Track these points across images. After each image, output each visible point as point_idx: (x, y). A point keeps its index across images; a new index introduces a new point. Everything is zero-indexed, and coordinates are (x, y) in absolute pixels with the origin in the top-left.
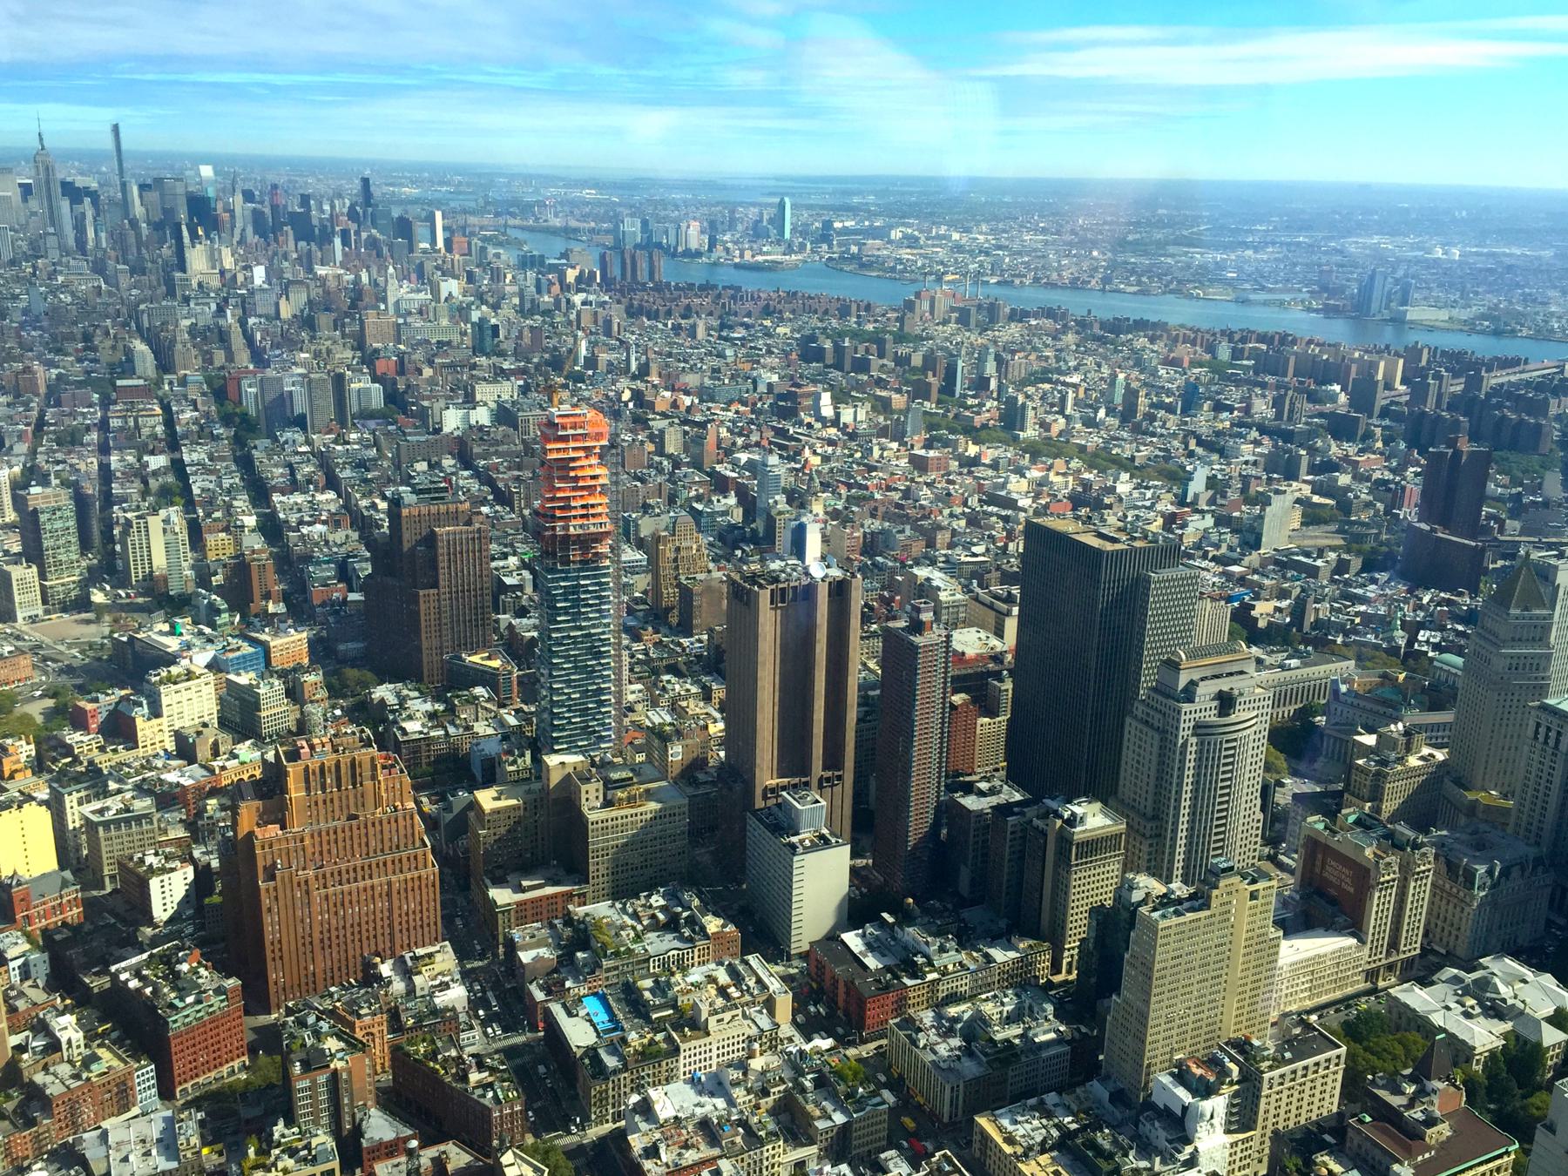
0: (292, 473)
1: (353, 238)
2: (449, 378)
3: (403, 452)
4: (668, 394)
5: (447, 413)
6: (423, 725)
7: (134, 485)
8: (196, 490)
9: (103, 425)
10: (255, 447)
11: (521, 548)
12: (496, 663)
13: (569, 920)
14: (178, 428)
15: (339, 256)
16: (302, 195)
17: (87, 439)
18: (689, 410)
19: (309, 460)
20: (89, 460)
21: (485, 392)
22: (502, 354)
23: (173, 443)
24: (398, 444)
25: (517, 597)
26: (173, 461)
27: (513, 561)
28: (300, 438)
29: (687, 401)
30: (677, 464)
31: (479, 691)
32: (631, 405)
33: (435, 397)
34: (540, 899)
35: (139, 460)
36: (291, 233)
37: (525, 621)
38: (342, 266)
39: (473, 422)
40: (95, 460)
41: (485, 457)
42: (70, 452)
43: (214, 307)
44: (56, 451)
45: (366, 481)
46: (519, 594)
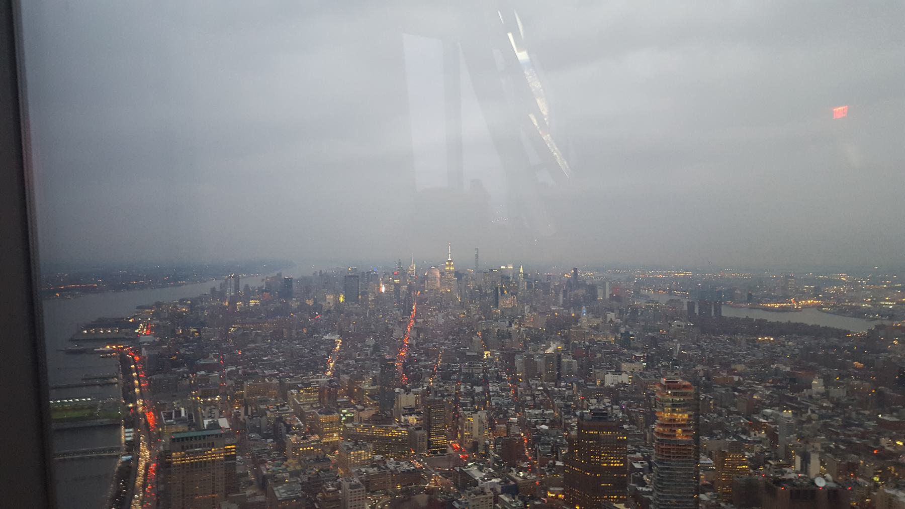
0: (534, 399)
7: (469, 399)
8: (493, 404)
10: (519, 386)
15: (561, 302)
17: (452, 377)
19: (542, 394)
20: (453, 386)
21: (625, 366)
23: (485, 382)
27: (639, 455)
29: (736, 378)
37: (644, 489)
38: (563, 306)
43: (508, 322)
44: (441, 382)
46: (641, 473)
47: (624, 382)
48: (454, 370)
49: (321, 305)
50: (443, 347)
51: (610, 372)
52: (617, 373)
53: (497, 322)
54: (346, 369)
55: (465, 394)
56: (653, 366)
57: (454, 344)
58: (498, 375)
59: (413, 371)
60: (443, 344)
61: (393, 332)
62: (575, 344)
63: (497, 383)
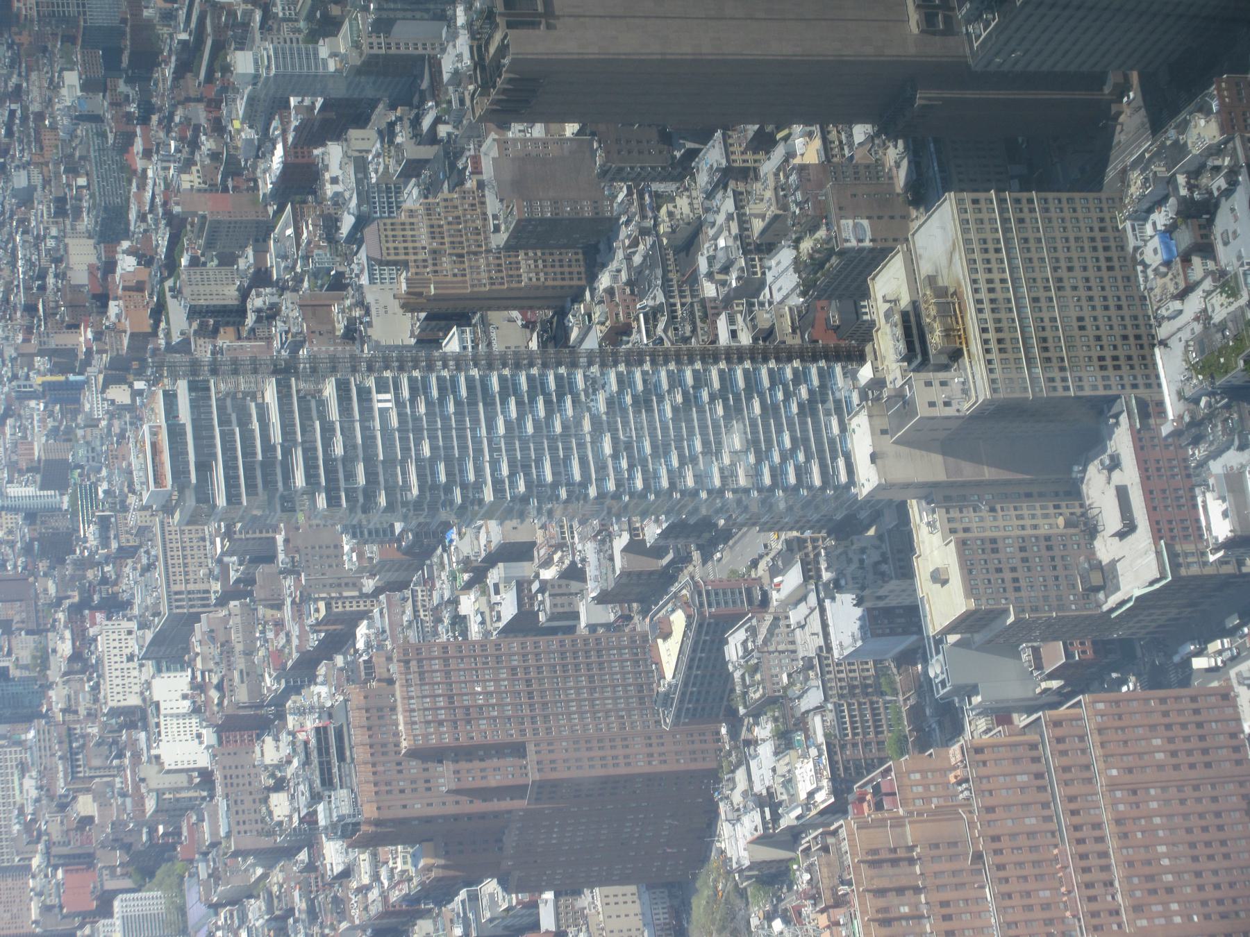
2: (96, 762)
3: (249, 842)
4: (113, 308)
5: (169, 761)
6: (805, 756)
11: (443, 589)
12: (678, 620)
13: (1193, 430)
18: (145, 259)
22: (43, 658)
24: (236, 854)
25: (542, 590)
27: (468, 604)
29: (126, 264)
30: (261, 278)
31: (733, 649)
32: (139, 385)
33: (137, 788)
34: (1148, 494)
37: (591, 571)
39: (186, 704)
41: (253, 677)
45: (312, 913)
46: (535, 586)
47: (187, 690)
51: (148, 750)
52: (153, 721)
56: (104, 580)
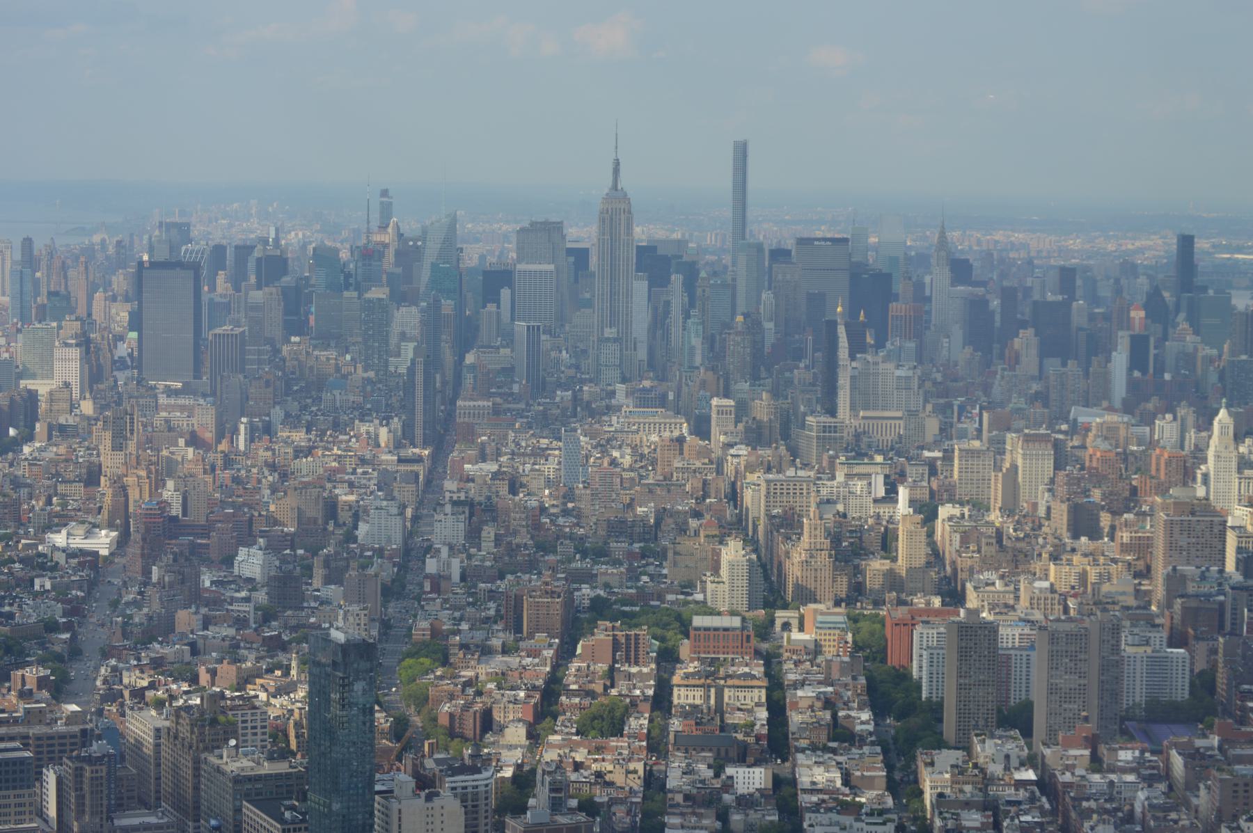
1: (1152, 351)
9: (661, 701)
14: (795, 719)
15: (1119, 389)
16: (1063, 269)
20: (632, 766)
26: (777, 781)
28: (1014, 746)
35: (717, 775)
36: (1034, 341)
38: (1127, 408)
40: (639, 767)
42: (599, 749)
44: (578, 744)
48: (638, 692)
49: (32, 396)
50: (586, 590)
53: (833, 478)
54: (152, 686)
55: (687, 797)
57: (638, 580)
58: (834, 716)
59: (452, 697)
60: (589, 578)
61: (356, 518)
62: (1183, 578)
63: (834, 751)
